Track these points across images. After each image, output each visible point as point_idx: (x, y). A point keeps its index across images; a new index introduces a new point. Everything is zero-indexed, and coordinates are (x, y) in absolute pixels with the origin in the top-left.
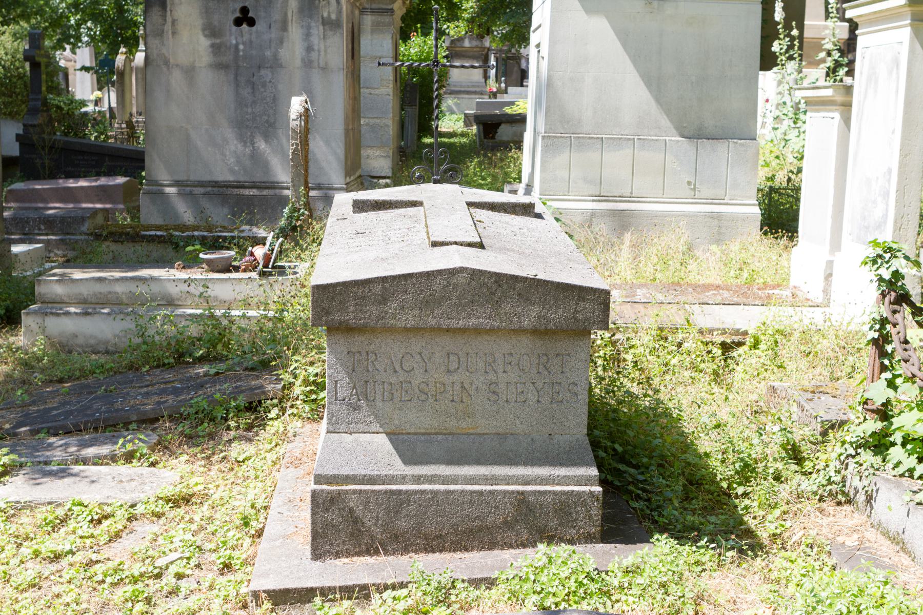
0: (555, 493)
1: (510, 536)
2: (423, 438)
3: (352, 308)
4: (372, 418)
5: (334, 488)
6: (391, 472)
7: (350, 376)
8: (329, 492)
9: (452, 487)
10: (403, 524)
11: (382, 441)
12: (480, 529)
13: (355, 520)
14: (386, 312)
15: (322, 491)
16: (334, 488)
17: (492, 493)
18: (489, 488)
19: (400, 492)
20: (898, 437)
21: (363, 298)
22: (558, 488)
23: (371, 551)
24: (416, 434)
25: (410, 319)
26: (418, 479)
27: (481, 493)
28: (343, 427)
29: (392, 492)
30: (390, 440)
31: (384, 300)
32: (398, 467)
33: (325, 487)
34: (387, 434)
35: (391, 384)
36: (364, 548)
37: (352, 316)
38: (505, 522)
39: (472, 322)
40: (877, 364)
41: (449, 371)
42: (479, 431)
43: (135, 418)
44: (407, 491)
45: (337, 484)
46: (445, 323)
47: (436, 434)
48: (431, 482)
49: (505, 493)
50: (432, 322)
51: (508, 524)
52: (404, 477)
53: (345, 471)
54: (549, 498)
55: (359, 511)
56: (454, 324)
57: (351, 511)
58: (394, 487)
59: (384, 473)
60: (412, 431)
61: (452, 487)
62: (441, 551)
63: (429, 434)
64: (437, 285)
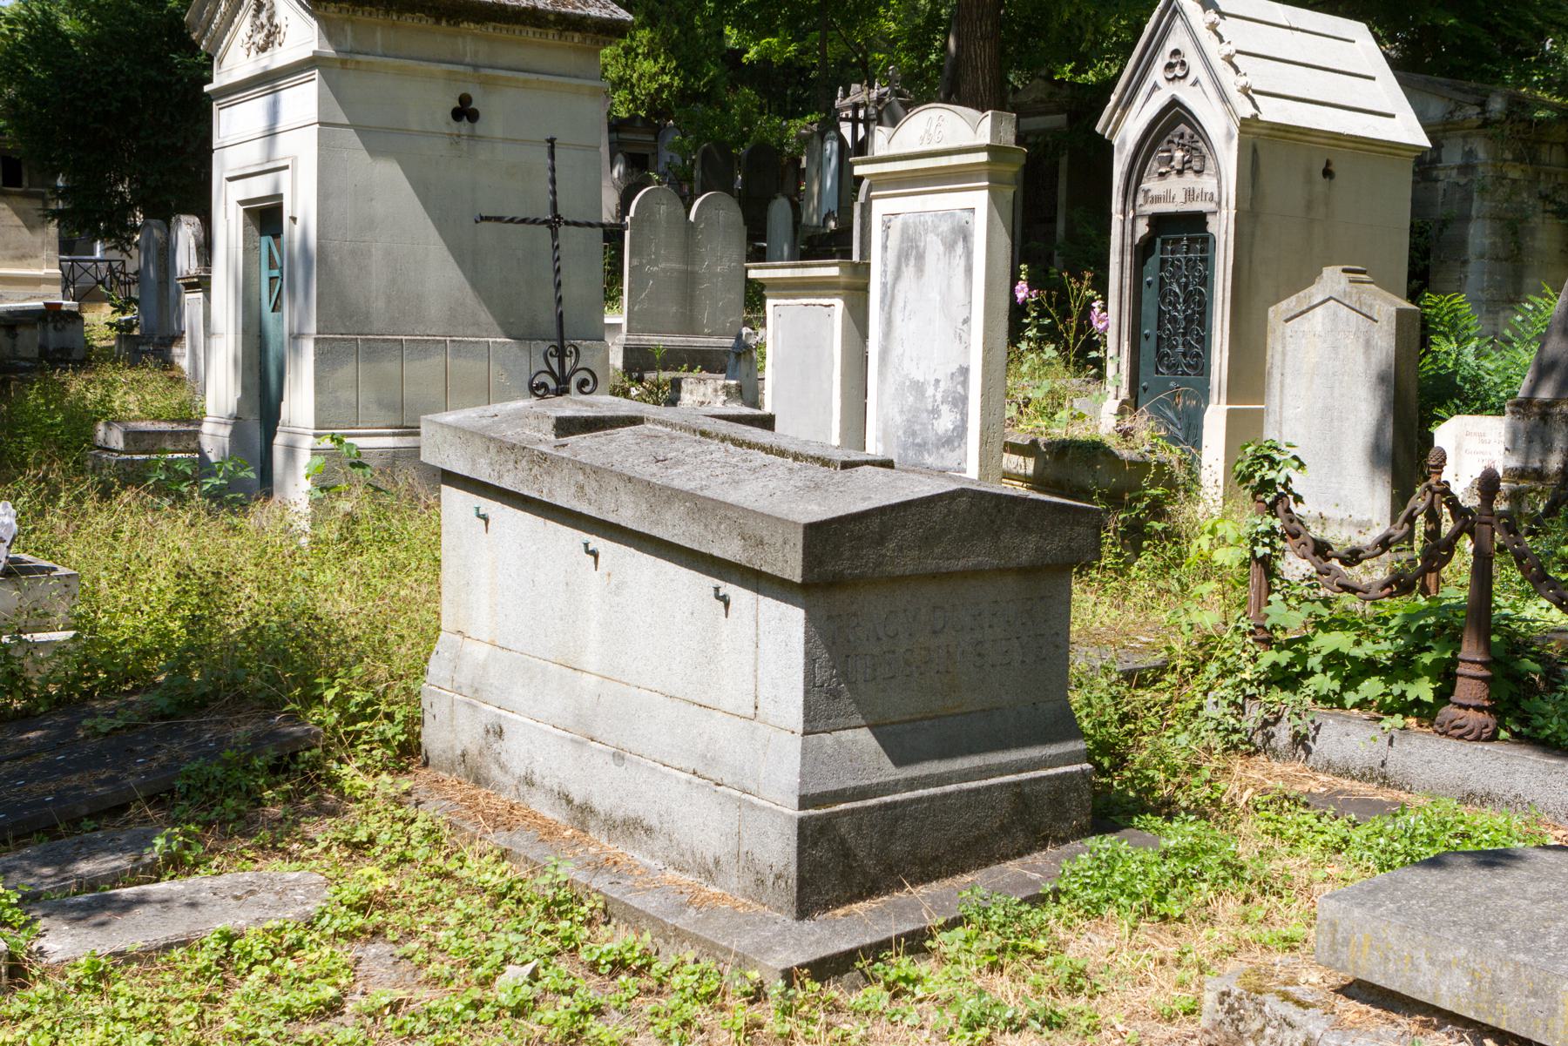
0: (1048, 778)
1: (1004, 844)
2: (908, 727)
3: (847, 554)
4: (853, 708)
5: (823, 811)
6: (882, 779)
7: (830, 652)
8: (818, 818)
9: (949, 788)
10: (898, 848)
11: (865, 737)
12: (977, 840)
13: (846, 853)
14: (884, 556)
15: (810, 817)
16: (823, 811)
17: (989, 788)
18: (984, 783)
19: (895, 804)
20: (1314, 662)
21: (860, 538)
22: (1051, 772)
23: (870, 889)
24: (899, 723)
25: (907, 564)
26: (911, 784)
27: (977, 791)
28: (821, 725)
29: (887, 806)
30: (875, 734)
31: (881, 540)
32: (890, 772)
33: (812, 812)
34: (871, 727)
35: (873, 656)
36: (856, 891)
37: (847, 564)
38: (1002, 827)
39: (971, 562)
40: (1264, 586)
41: (935, 632)
42: (964, 709)
43: (85, 810)
44: (903, 802)
45: (825, 805)
46: (945, 565)
47: (921, 719)
48: (925, 786)
49: (1002, 785)
50: (931, 564)
51: (1004, 829)
52: (897, 782)
53: (833, 786)
54: (1043, 787)
55: (851, 839)
56: (959, 565)
57: (843, 841)
58: (888, 799)
59: (875, 781)
60: (896, 719)
61: (949, 788)
62: (937, 878)
63: (914, 721)
64: (875, 524)
